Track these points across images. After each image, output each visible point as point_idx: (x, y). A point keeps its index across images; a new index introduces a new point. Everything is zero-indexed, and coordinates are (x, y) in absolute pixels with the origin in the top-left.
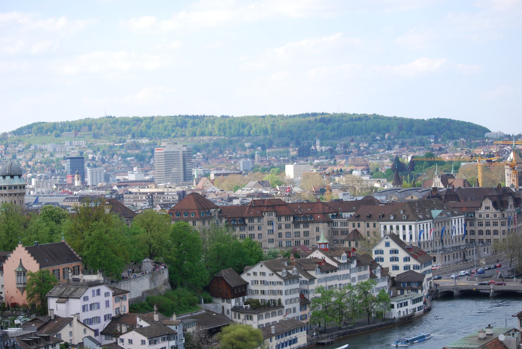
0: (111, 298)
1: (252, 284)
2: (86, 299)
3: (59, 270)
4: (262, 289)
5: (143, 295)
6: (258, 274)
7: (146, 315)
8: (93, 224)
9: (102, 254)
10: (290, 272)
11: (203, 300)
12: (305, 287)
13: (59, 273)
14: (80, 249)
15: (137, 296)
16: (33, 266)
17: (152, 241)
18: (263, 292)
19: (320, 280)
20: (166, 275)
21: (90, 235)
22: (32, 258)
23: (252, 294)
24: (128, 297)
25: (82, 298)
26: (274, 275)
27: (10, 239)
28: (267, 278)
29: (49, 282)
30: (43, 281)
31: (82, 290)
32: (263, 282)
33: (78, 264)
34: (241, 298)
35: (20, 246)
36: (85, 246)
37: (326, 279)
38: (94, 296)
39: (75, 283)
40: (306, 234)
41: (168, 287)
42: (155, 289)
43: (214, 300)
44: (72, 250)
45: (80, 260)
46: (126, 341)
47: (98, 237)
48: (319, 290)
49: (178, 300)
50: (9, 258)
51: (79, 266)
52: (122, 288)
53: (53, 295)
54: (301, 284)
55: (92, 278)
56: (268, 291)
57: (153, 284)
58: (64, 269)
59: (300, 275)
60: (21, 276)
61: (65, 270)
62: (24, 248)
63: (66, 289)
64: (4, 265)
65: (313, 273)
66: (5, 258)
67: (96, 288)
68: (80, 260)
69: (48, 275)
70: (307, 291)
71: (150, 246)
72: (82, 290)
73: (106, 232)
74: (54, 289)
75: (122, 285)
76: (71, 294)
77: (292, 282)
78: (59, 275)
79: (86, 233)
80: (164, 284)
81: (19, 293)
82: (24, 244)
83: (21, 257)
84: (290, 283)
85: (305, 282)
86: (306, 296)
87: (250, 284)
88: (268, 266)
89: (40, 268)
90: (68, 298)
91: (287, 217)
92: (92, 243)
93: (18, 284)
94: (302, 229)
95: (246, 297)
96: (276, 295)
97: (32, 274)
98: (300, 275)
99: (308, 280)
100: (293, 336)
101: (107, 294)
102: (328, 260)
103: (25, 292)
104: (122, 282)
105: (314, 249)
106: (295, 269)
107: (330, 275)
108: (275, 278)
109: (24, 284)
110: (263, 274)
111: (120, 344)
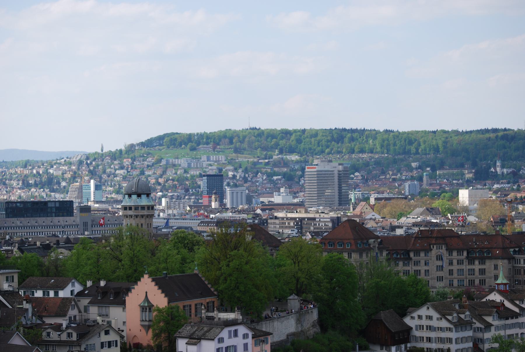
0: (250, 341)
1: (417, 330)
2: (221, 340)
3: (190, 306)
4: (428, 336)
5: (287, 338)
6: (424, 318)
8: (232, 253)
9: (242, 288)
10: (462, 316)
11: (357, 346)
12: (479, 335)
13: (190, 309)
14: (215, 282)
15: (281, 339)
16: (160, 300)
17: (300, 275)
18: (429, 340)
19: (497, 328)
20: (315, 315)
21: (228, 266)
22: (160, 291)
23: (417, 341)
24: (270, 339)
25: (216, 340)
26: (443, 319)
27: (135, 268)
28: (435, 323)
29: (178, 321)
30: (172, 319)
31: (217, 331)
32: (430, 328)
33: (213, 300)
34: (403, 346)
35: (146, 276)
36: (222, 278)
37: (505, 327)
38: (230, 337)
39: (208, 321)
40: (482, 272)
41: (318, 329)
42: (302, 331)
43: (372, 347)
44: (206, 282)
45: (215, 295)
47: (237, 269)
48: (496, 339)
49: (329, 345)
50: (133, 290)
51: (213, 302)
52: (264, 330)
53: (182, 335)
54: (474, 331)
55: (228, 317)
56: (435, 338)
57: (299, 325)
58: (196, 305)
59: (474, 321)
60: (146, 311)
61: (198, 306)
62: (150, 280)
63: (198, 328)
64: (127, 298)
65: (489, 319)
66: (128, 290)
67: (233, 328)
68: (215, 295)
69: (178, 311)
70: (482, 341)
71: (298, 280)
72: (215, 330)
73: (247, 263)
74: (184, 327)
75: (264, 326)
76: (204, 334)
77: (464, 328)
78: (190, 312)
79: (223, 263)
80: (313, 326)
81: (144, 331)
82: (151, 274)
83: (146, 290)
84: (462, 330)
85: (480, 330)
86: (481, 346)
87: (414, 329)
88: (436, 309)
89: (169, 303)
90: (200, 339)
91: (460, 251)
92: (230, 275)
93: (143, 321)
94: (477, 266)
95: (409, 345)
96: (444, 343)
97: (159, 310)
98: (474, 321)
99: (483, 327)
101: (245, 336)
102: (507, 304)
103: (151, 331)
104: (264, 323)
105: (491, 291)
106: (468, 313)
107: (510, 321)
108: (444, 324)
109: (150, 321)
110: (430, 318)
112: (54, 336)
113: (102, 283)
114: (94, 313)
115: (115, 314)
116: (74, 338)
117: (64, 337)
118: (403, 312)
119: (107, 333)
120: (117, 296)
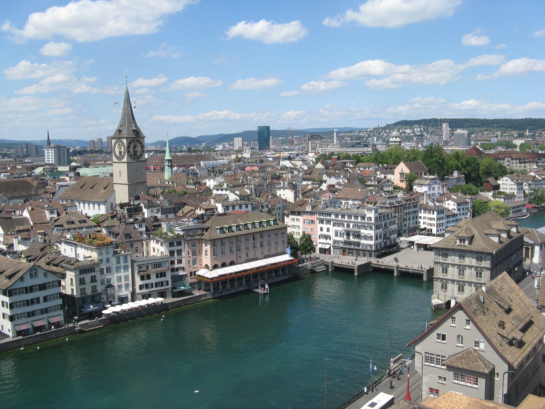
7: (456, 194)
16: (407, 171)
46: (447, 204)
66: (394, 168)
83: (402, 168)
91: (516, 159)
94: (523, 165)
100: (520, 208)
102: (537, 176)
108: (512, 183)
111: (444, 205)
112: (369, 183)
113: (385, 165)
114: (382, 176)
115: (389, 177)
116: (376, 183)
117: (373, 183)
118: (497, 179)
119: (388, 181)
120: (391, 170)
